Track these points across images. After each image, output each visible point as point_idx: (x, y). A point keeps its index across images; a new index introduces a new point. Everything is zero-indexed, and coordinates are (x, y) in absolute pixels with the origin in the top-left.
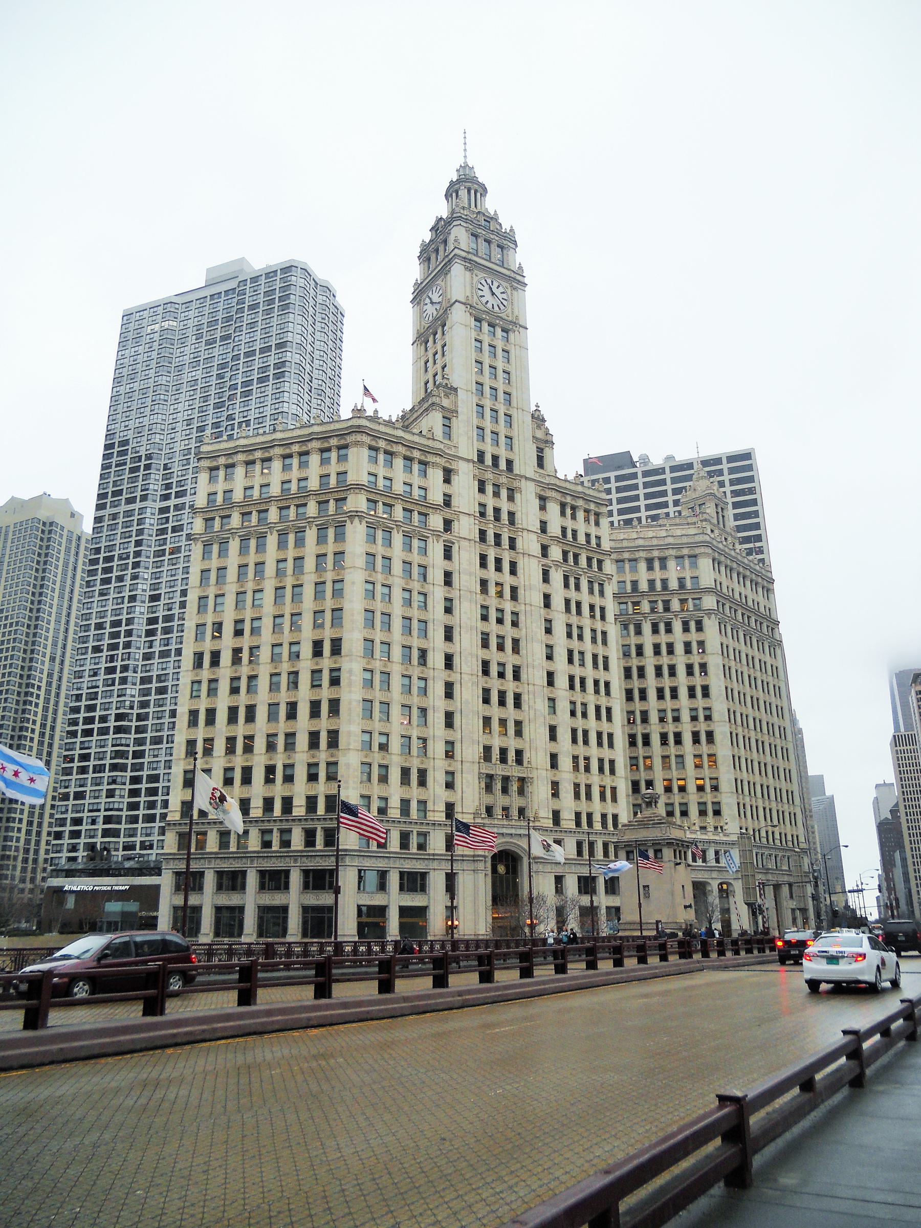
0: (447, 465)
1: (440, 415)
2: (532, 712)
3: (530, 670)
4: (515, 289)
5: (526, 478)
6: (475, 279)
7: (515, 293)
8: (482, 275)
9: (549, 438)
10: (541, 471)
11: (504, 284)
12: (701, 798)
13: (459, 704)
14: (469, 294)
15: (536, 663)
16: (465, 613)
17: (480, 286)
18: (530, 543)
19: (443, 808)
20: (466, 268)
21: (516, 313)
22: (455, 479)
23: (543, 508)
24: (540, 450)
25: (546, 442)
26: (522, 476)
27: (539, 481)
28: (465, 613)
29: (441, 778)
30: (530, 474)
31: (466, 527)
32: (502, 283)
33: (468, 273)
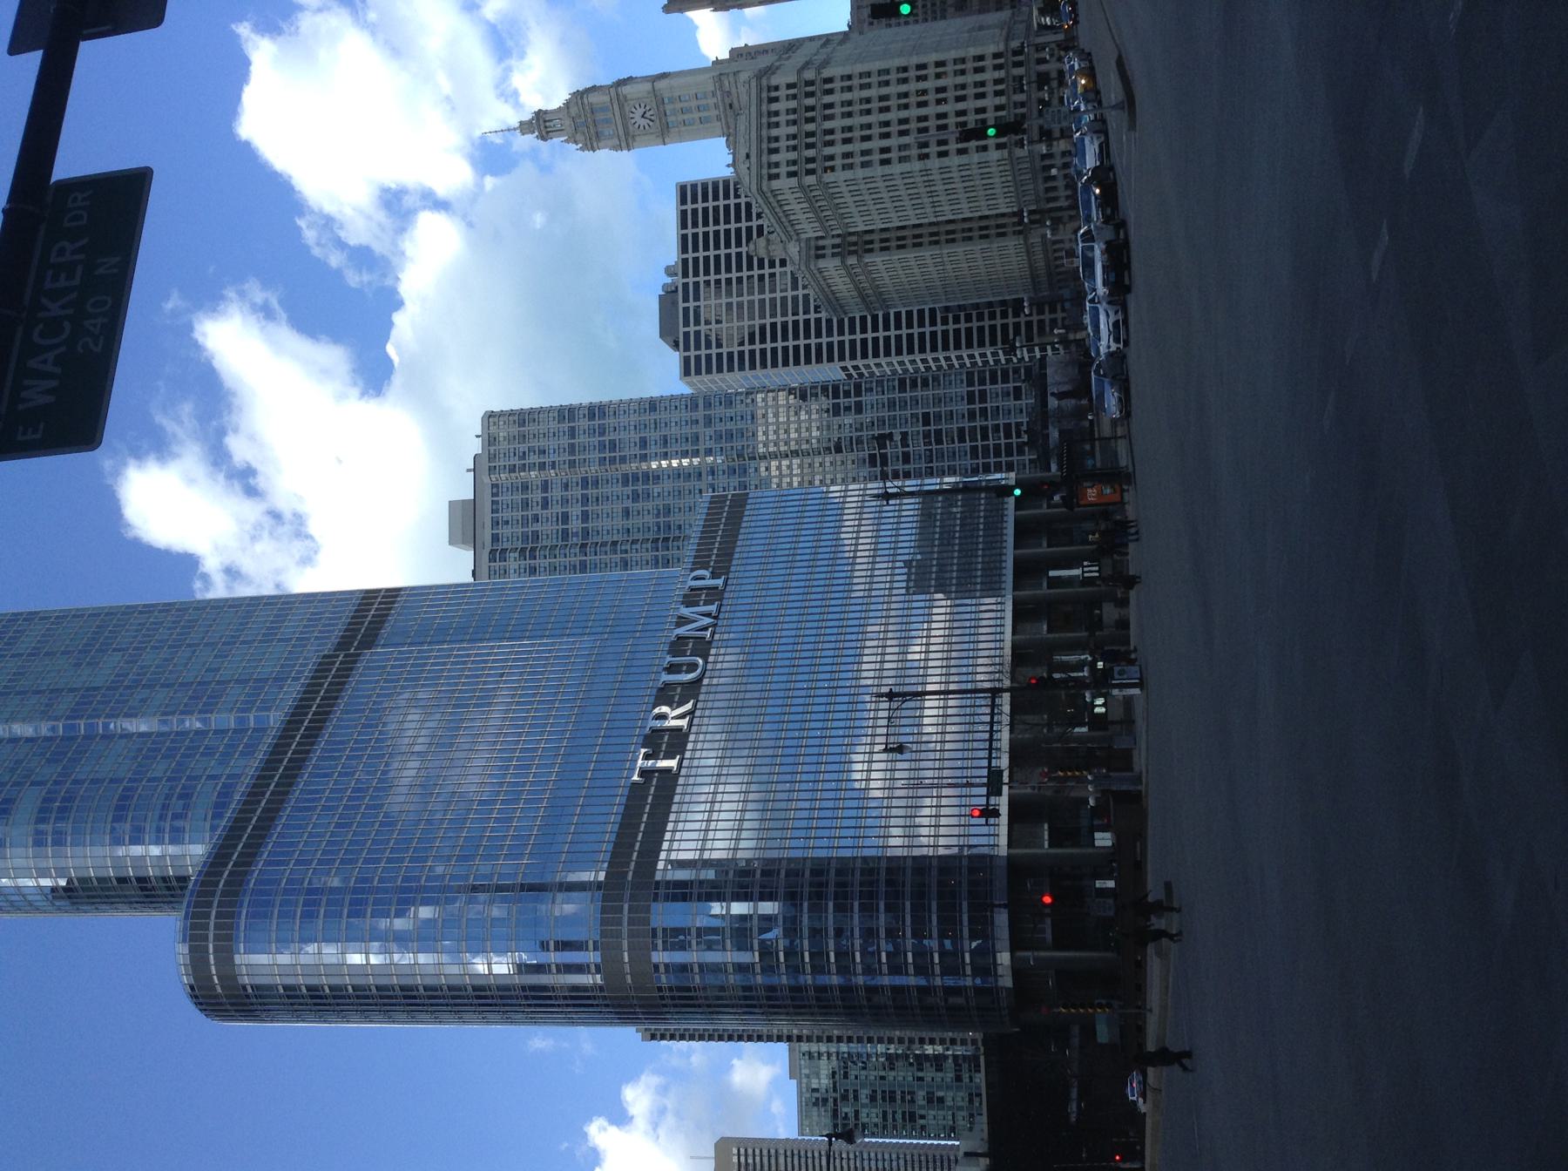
4: (625, 97)
6: (637, 133)
7: (629, 97)
8: (631, 128)
11: (627, 109)
14: (653, 137)
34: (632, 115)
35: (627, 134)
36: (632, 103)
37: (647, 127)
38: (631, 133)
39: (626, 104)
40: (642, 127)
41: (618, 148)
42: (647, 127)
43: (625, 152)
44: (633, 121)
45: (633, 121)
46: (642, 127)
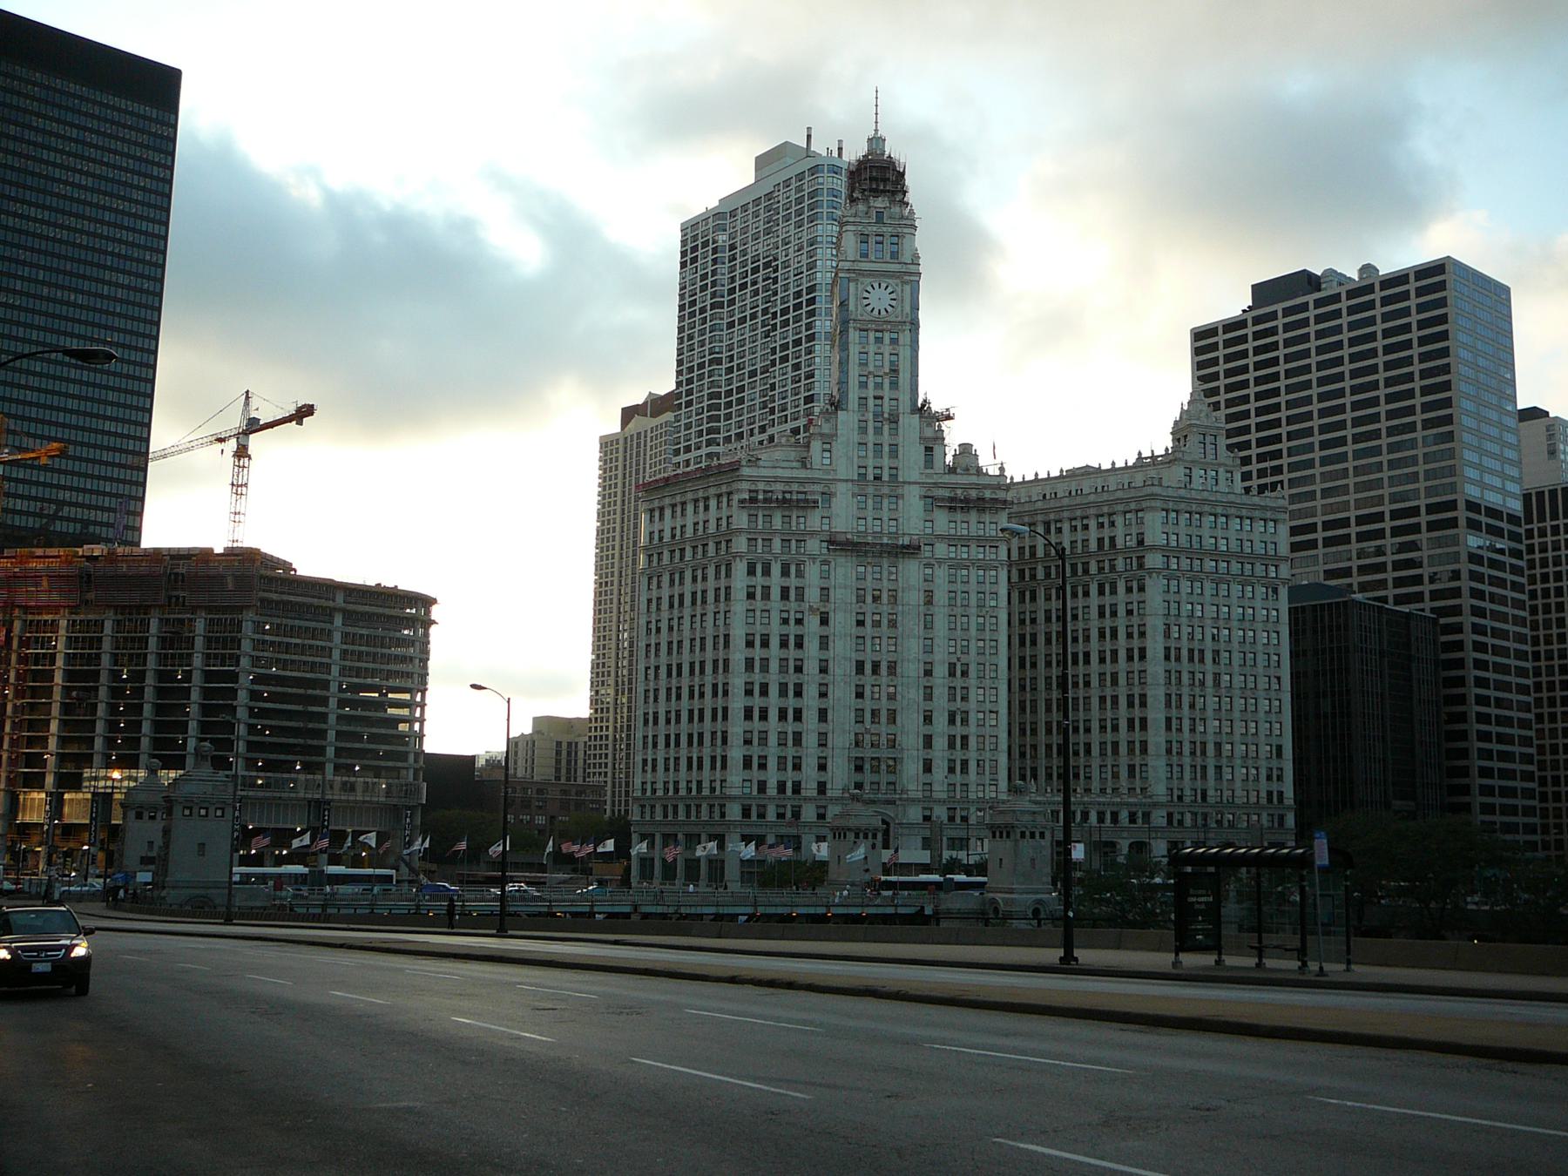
0: (826, 490)
1: (820, 443)
2: (905, 702)
3: (905, 664)
4: (904, 283)
5: (909, 483)
6: (860, 287)
8: (869, 280)
9: (939, 434)
10: (928, 471)
12: (1131, 760)
13: (831, 701)
15: (911, 658)
19: (815, 785)
24: (929, 449)
25: (936, 439)
26: (904, 482)
27: (923, 483)
29: (814, 762)
30: (915, 477)
32: (890, 281)
39: (898, 281)
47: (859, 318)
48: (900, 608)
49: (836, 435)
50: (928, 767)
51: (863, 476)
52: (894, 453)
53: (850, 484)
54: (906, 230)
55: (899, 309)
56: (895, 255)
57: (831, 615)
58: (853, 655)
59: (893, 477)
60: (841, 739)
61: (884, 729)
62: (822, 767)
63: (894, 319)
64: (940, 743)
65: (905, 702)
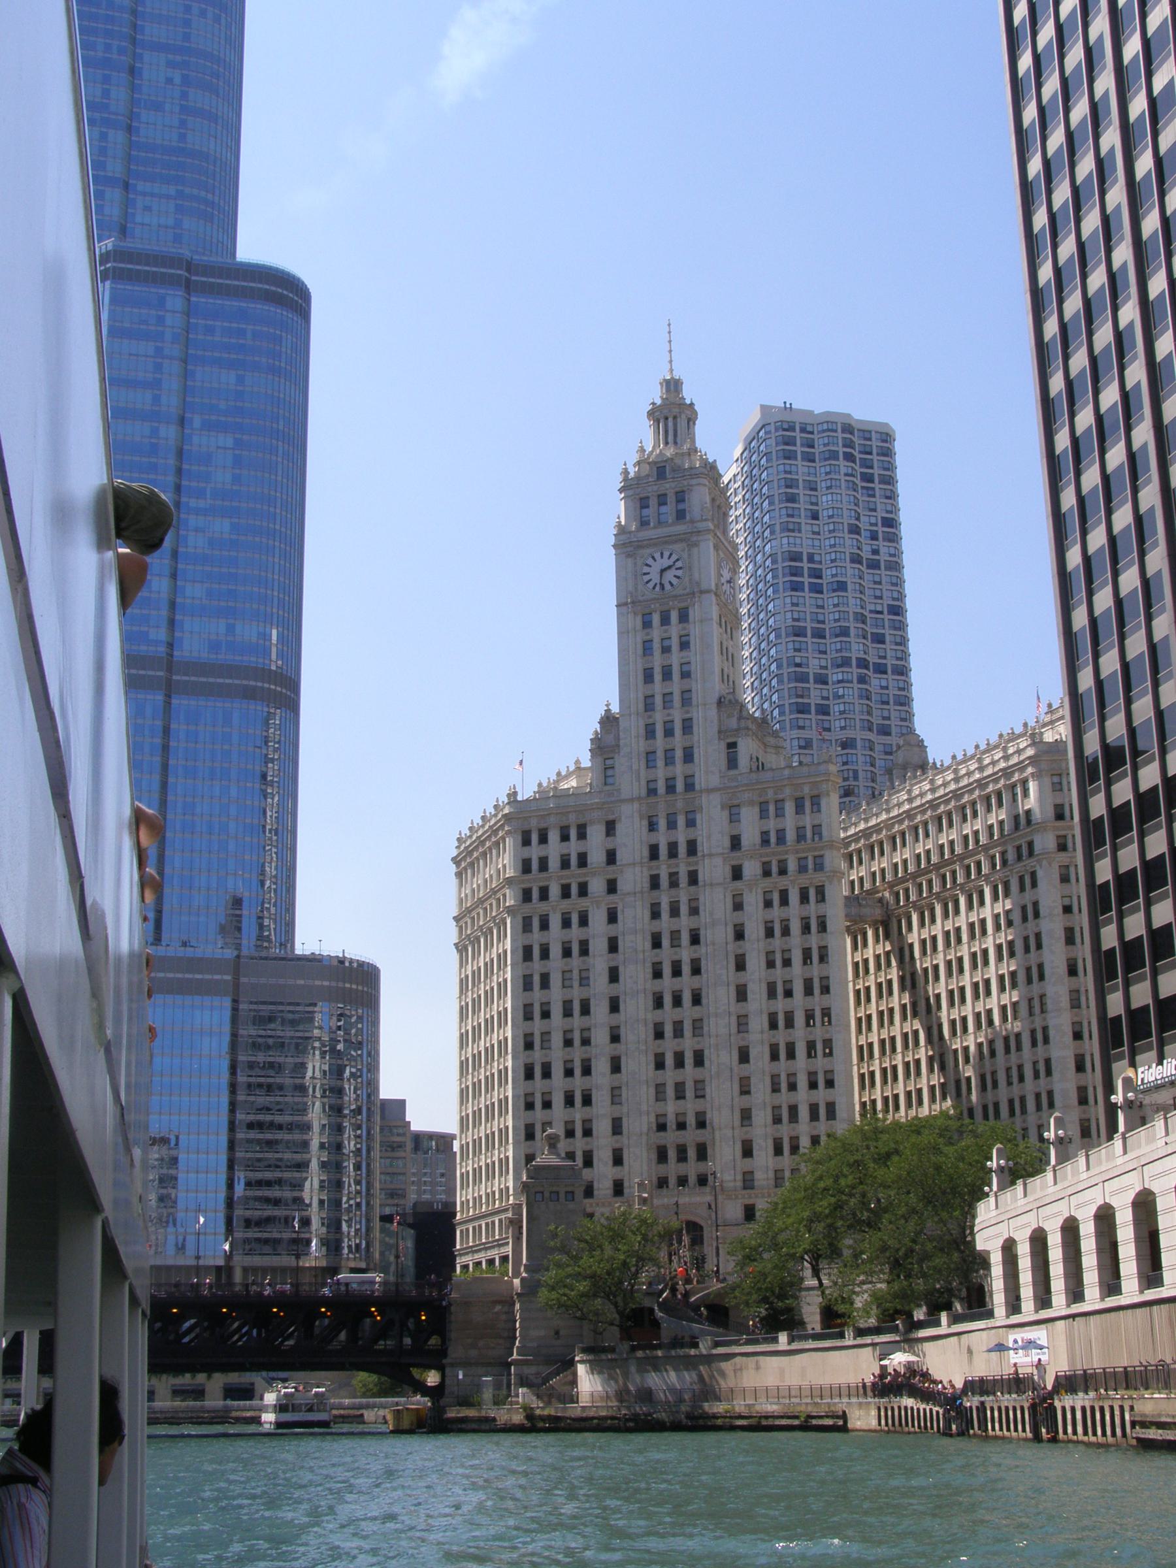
2: (714, 1069)
3: (712, 1020)
4: (696, 544)
7: (695, 550)
8: (648, 551)
11: (677, 547)
16: (631, 977)
17: (666, 554)
18: (713, 869)
20: (629, 556)
21: (696, 576)
22: (620, 828)
23: (734, 818)
26: (701, 791)
28: (631, 977)
31: (633, 878)
33: (630, 560)
34: (666, 554)
35: (641, 545)
36: (685, 556)
37: (646, 578)
38: (641, 551)
39: (684, 545)
40: (646, 569)
41: (621, 530)
42: (646, 578)
43: (612, 540)
44: (657, 556)
45: (657, 556)
46: (646, 569)
47: (641, 599)
48: (703, 950)
49: (618, 746)
50: (747, 1152)
51: (652, 792)
52: (688, 757)
53: (636, 805)
54: (694, 482)
55: (687, 579)
56: (681, 515)
57: (621, 969)
58: (649, 1016)
59: (689, 786)
60: (639, 1125)
61: (689, 1106)
62: (618, 1160)
63: (681, 592)
64: (762, 1117)
65: (714, 1069)
